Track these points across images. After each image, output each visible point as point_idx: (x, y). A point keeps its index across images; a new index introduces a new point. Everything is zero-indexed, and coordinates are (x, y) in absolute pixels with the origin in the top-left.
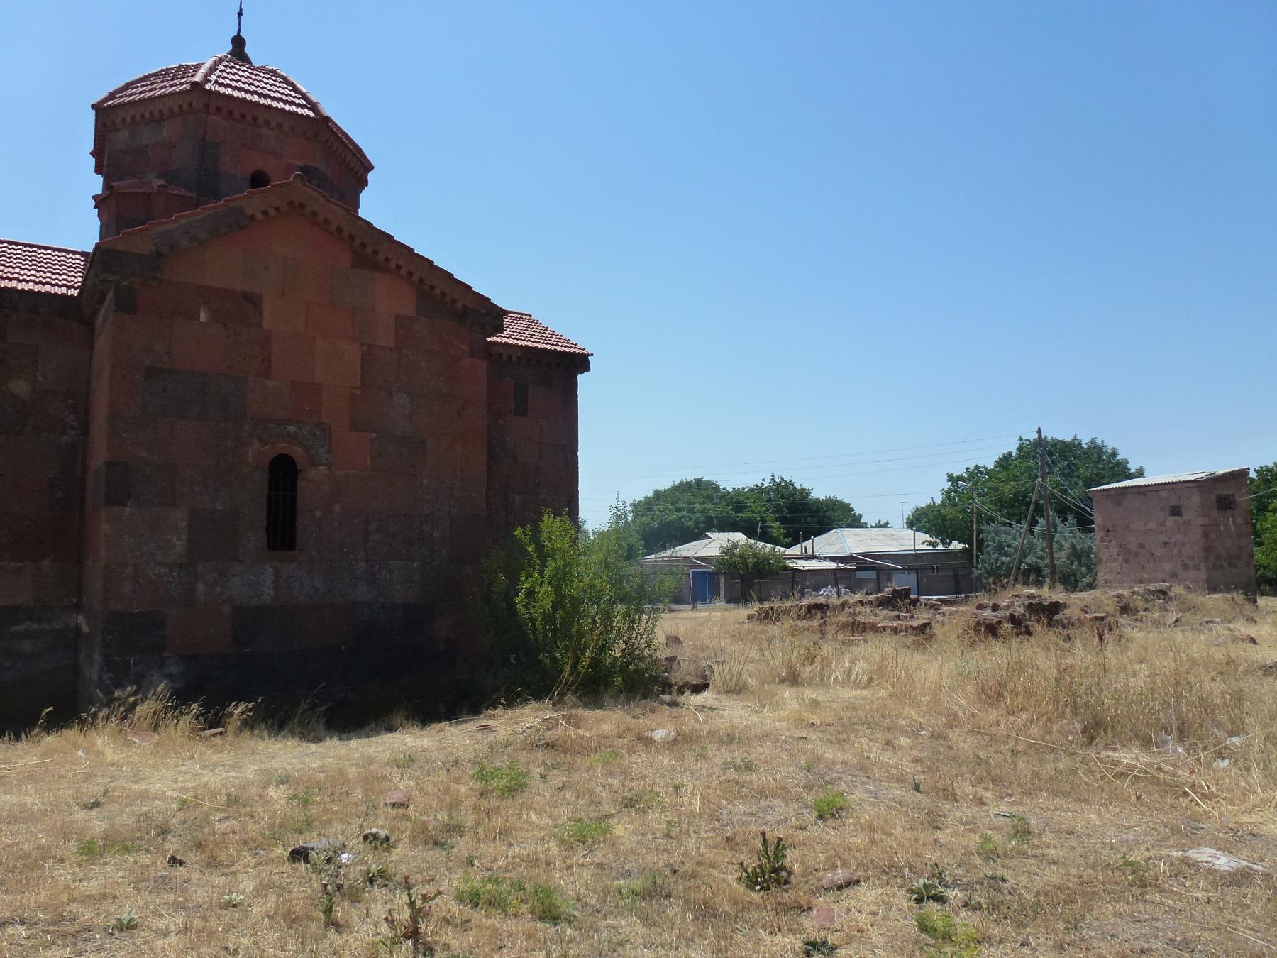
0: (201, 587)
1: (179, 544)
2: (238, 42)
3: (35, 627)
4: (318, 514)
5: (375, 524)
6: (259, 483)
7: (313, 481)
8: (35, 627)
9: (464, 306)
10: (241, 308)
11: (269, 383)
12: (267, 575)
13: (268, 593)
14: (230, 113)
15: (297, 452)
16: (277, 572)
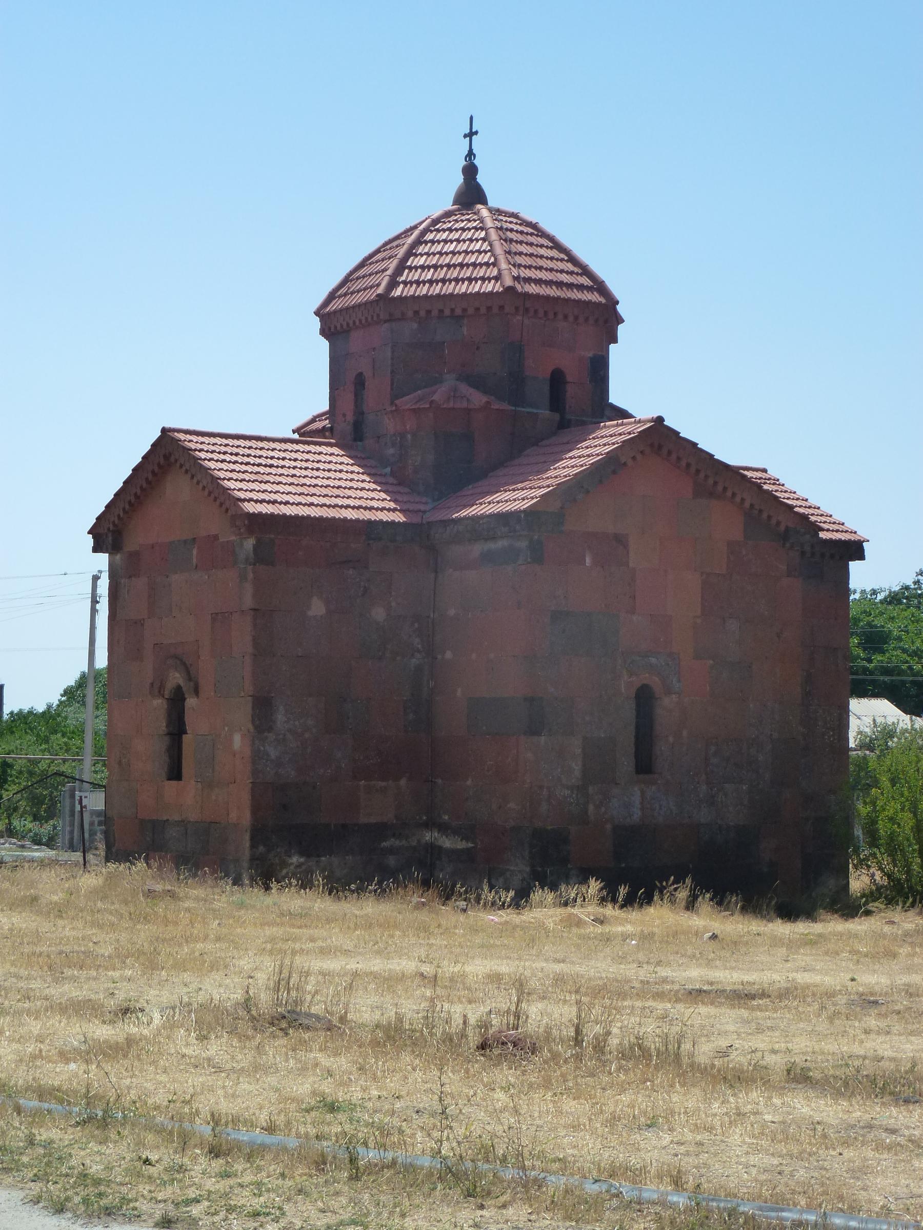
0: (591, 807)
1: (577, 768)
2: (470, 171)
3: (398, 843)
4: (671, 739)
5: (713, 749)
6: (629, 712)
7: (666, 708)
8: (398, 843)
9: (787, 527)
10: (613, 547)
11: (635, 618)
12: (637, 799)
13: (637, 815)
14: (536, 311)
15: (655, 682)
16: (643, 793)
